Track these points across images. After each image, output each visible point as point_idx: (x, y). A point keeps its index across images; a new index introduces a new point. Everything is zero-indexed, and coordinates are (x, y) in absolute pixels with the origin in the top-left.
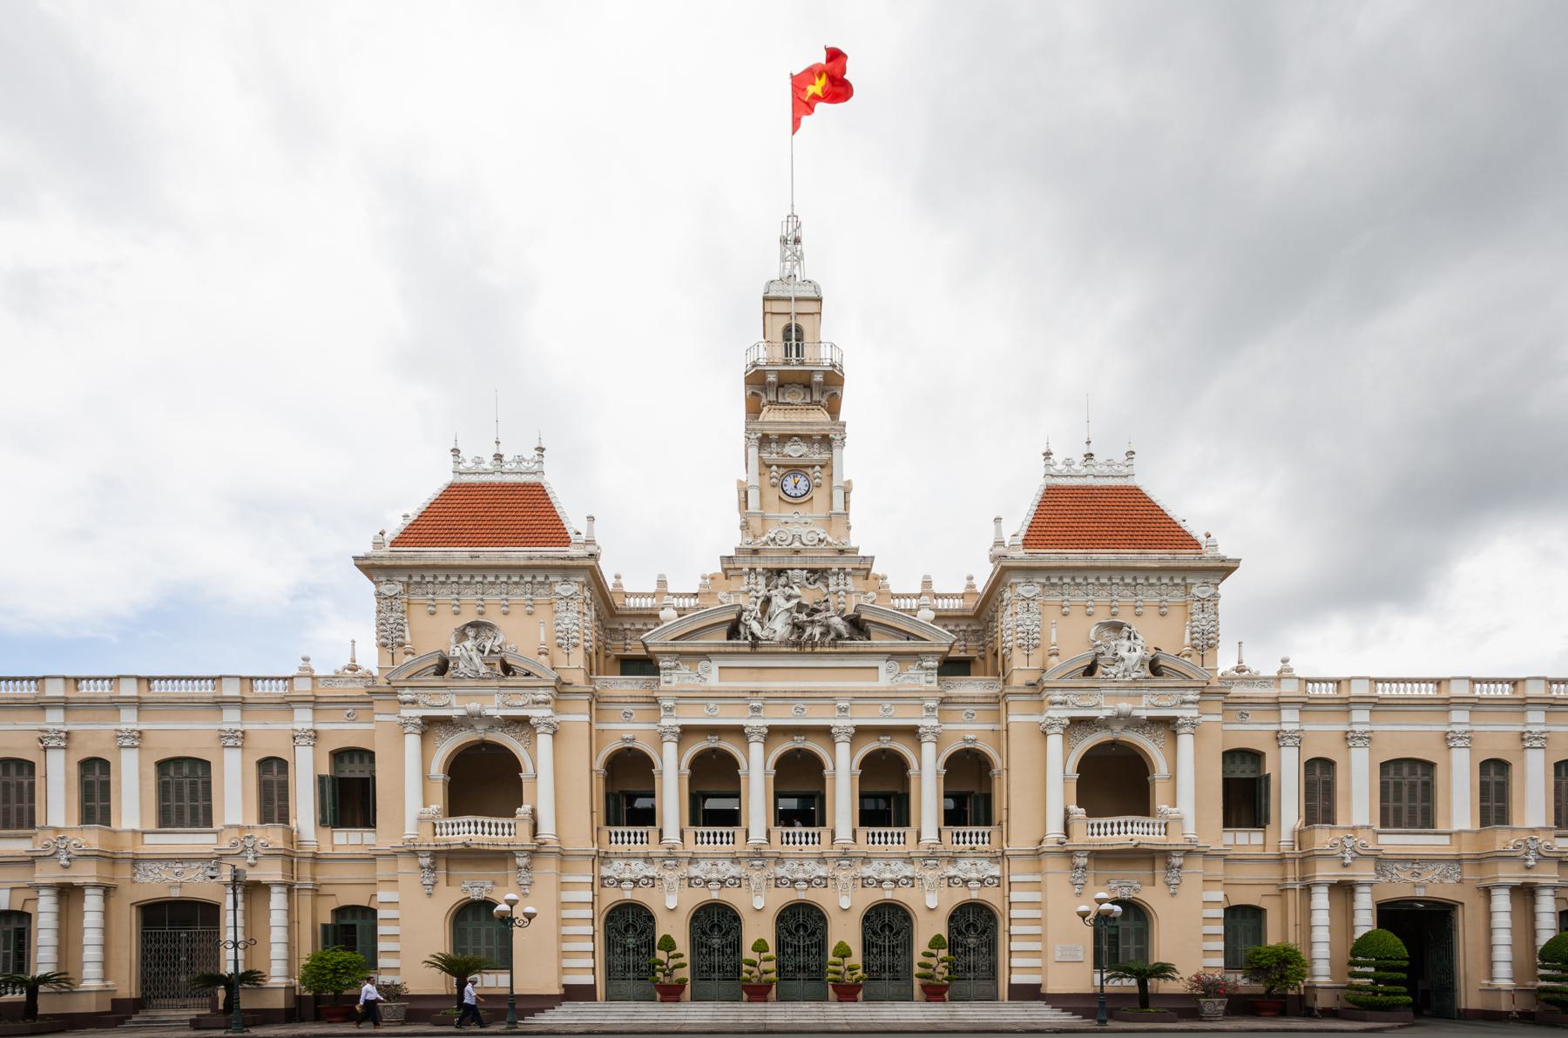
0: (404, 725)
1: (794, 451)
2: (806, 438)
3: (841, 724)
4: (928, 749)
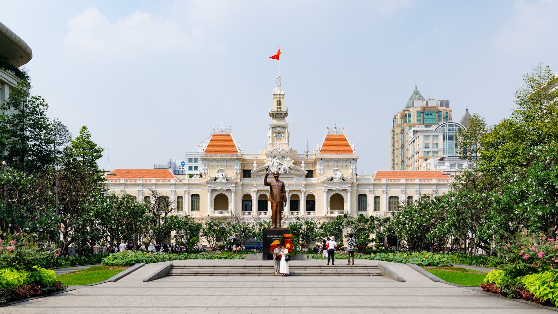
1: (278, 130)
4: (303, 195)
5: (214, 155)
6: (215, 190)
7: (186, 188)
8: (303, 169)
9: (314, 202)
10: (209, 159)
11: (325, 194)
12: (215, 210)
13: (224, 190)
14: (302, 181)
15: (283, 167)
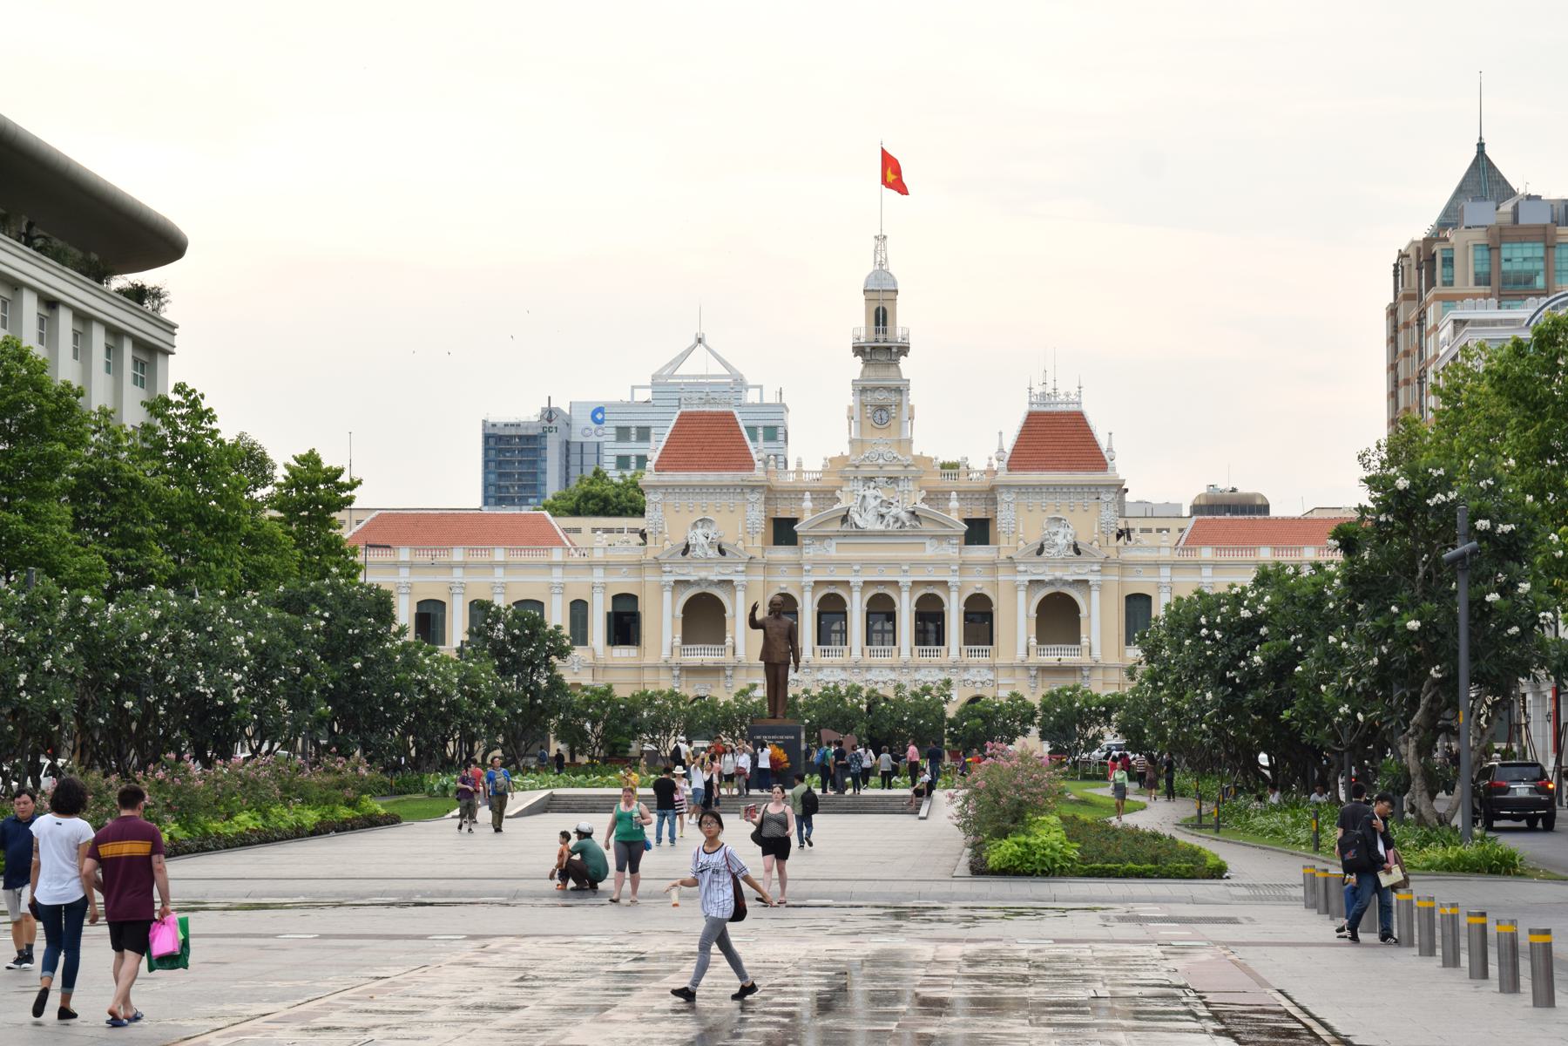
1: (880, 397)
2: (888, 389)
3: (905, 580)
4: (954, 596)
5: (681, 477)
6: (687, 582)
7: (598, 576)
8: (954, 516)
9: (988, 616)
10: (666, 487)
12: (685, 640)
13: (711, 583)
14: (952, 551)
15: (894, 511)
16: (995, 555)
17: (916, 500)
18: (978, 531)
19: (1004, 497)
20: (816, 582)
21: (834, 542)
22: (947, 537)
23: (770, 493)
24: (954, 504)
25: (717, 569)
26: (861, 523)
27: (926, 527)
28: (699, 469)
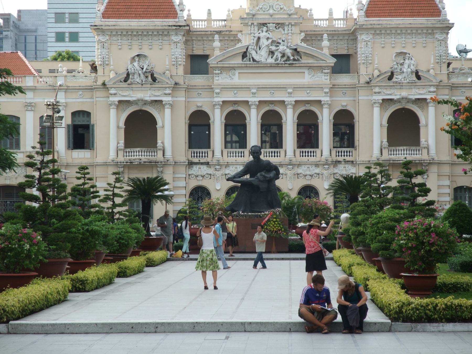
0: (111, 105)
4: (326, 111)
6: (128, 102)
8: (326, 51)
9: (351, 127)
10: (111, 31)
11: (376, 110)
13: (145, 103)
14: (323, 79)
16: (356, 81)
17: (297, 40)
18: (343, 63)
19: (362, 37)
20: (223, 102)
21: (237, 72)
22: (321, 68)
23: (188, 32)
24: (326, 43)
25: (149, 92)
26: (257, 58)
27: (305, 60)
28: (136, 17)
